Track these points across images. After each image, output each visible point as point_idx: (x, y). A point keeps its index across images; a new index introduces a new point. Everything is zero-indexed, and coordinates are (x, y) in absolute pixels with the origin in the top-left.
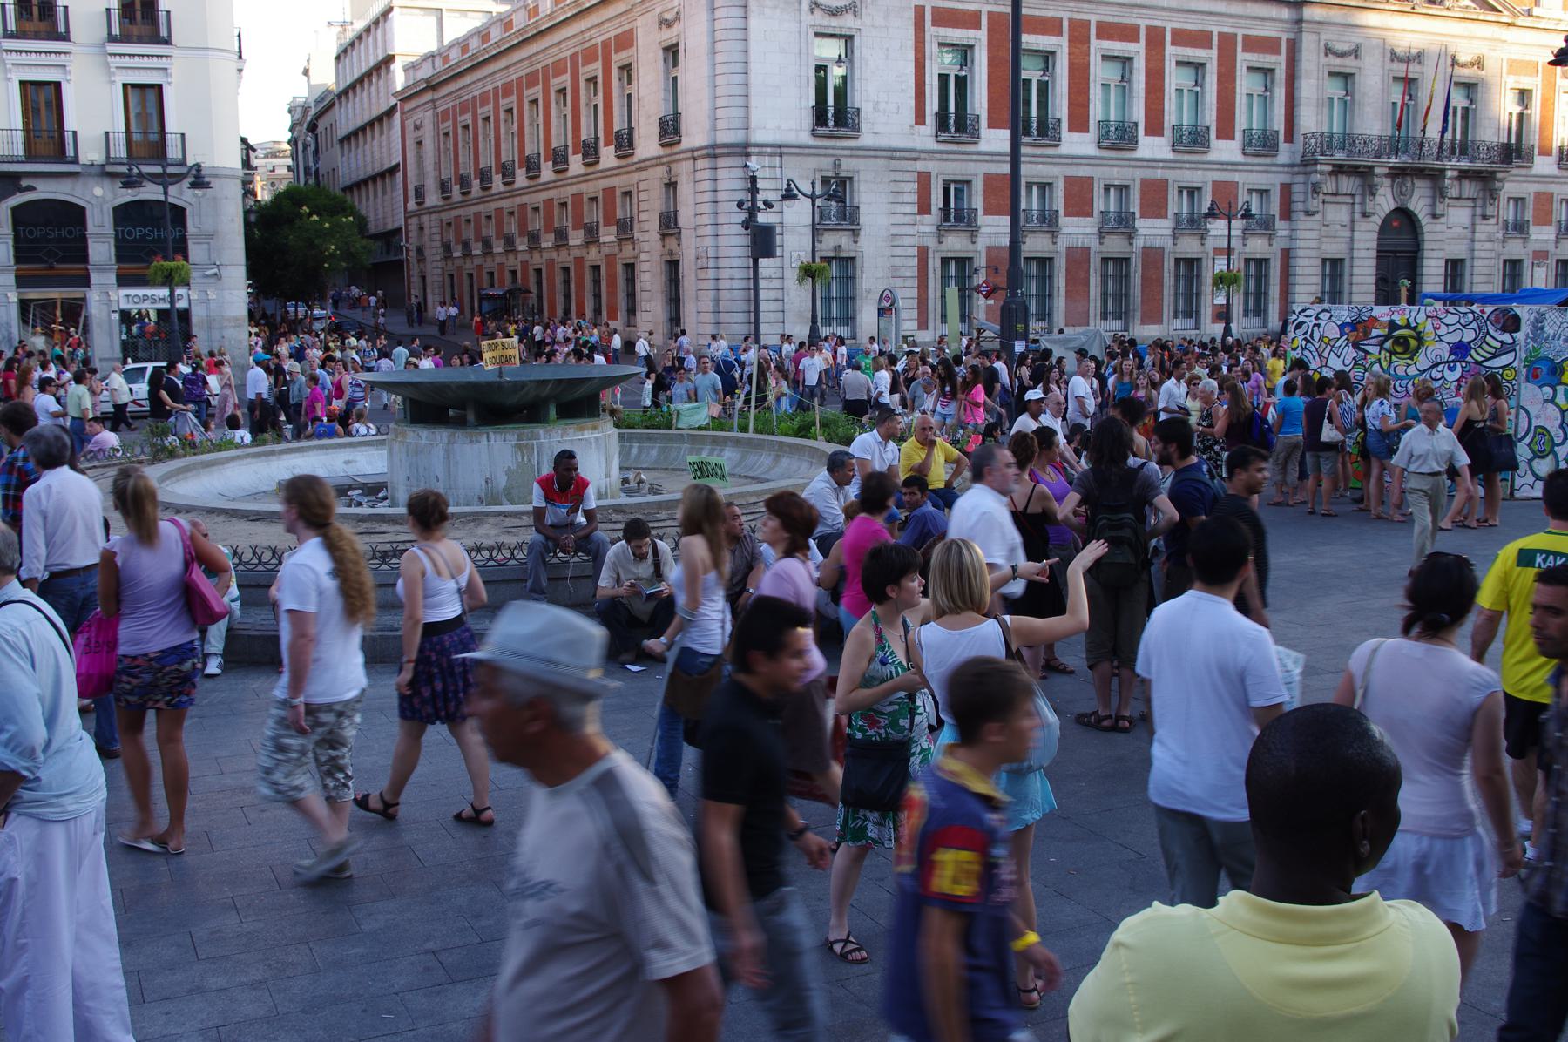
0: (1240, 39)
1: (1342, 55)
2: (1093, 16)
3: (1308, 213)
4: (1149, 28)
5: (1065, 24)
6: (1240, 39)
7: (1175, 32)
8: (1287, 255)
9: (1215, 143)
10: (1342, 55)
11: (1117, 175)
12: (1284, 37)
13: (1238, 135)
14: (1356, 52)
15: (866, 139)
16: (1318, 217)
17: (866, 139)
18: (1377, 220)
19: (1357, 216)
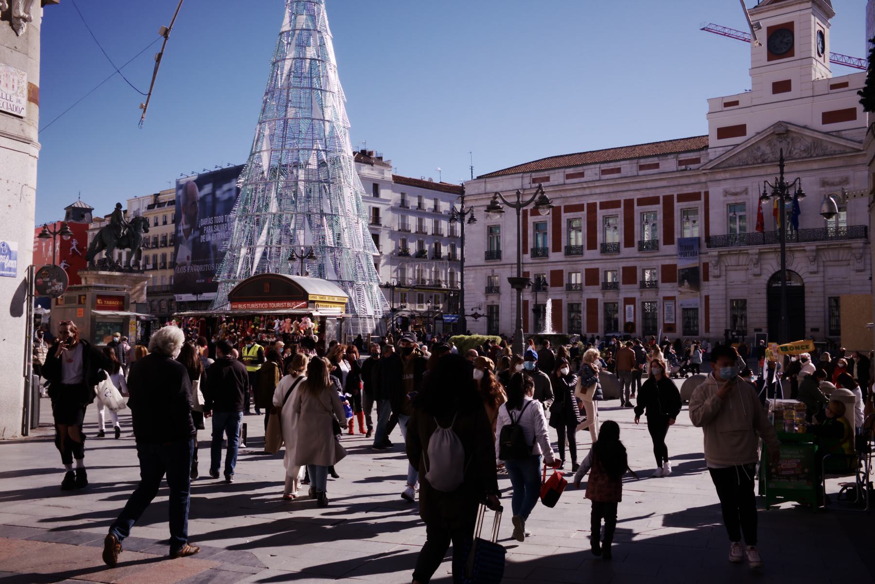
0: (675, 196)
1: (736, 194)
2: (598, 200)
3: (715, 277)
4: (588, 204)
5: (585, 206)
6: (675, 196)
7: (639, 200)
8: (707, 298)
9: (551, 254)
10: (736, 194)
11: (609, 266)
12: (703, 191)
13: (599, 246)
14: (746, 191)
15: (504, 261)
16: (723, 278)
17: (504, 261)
18: (765, 278)
19: (751, 277)
